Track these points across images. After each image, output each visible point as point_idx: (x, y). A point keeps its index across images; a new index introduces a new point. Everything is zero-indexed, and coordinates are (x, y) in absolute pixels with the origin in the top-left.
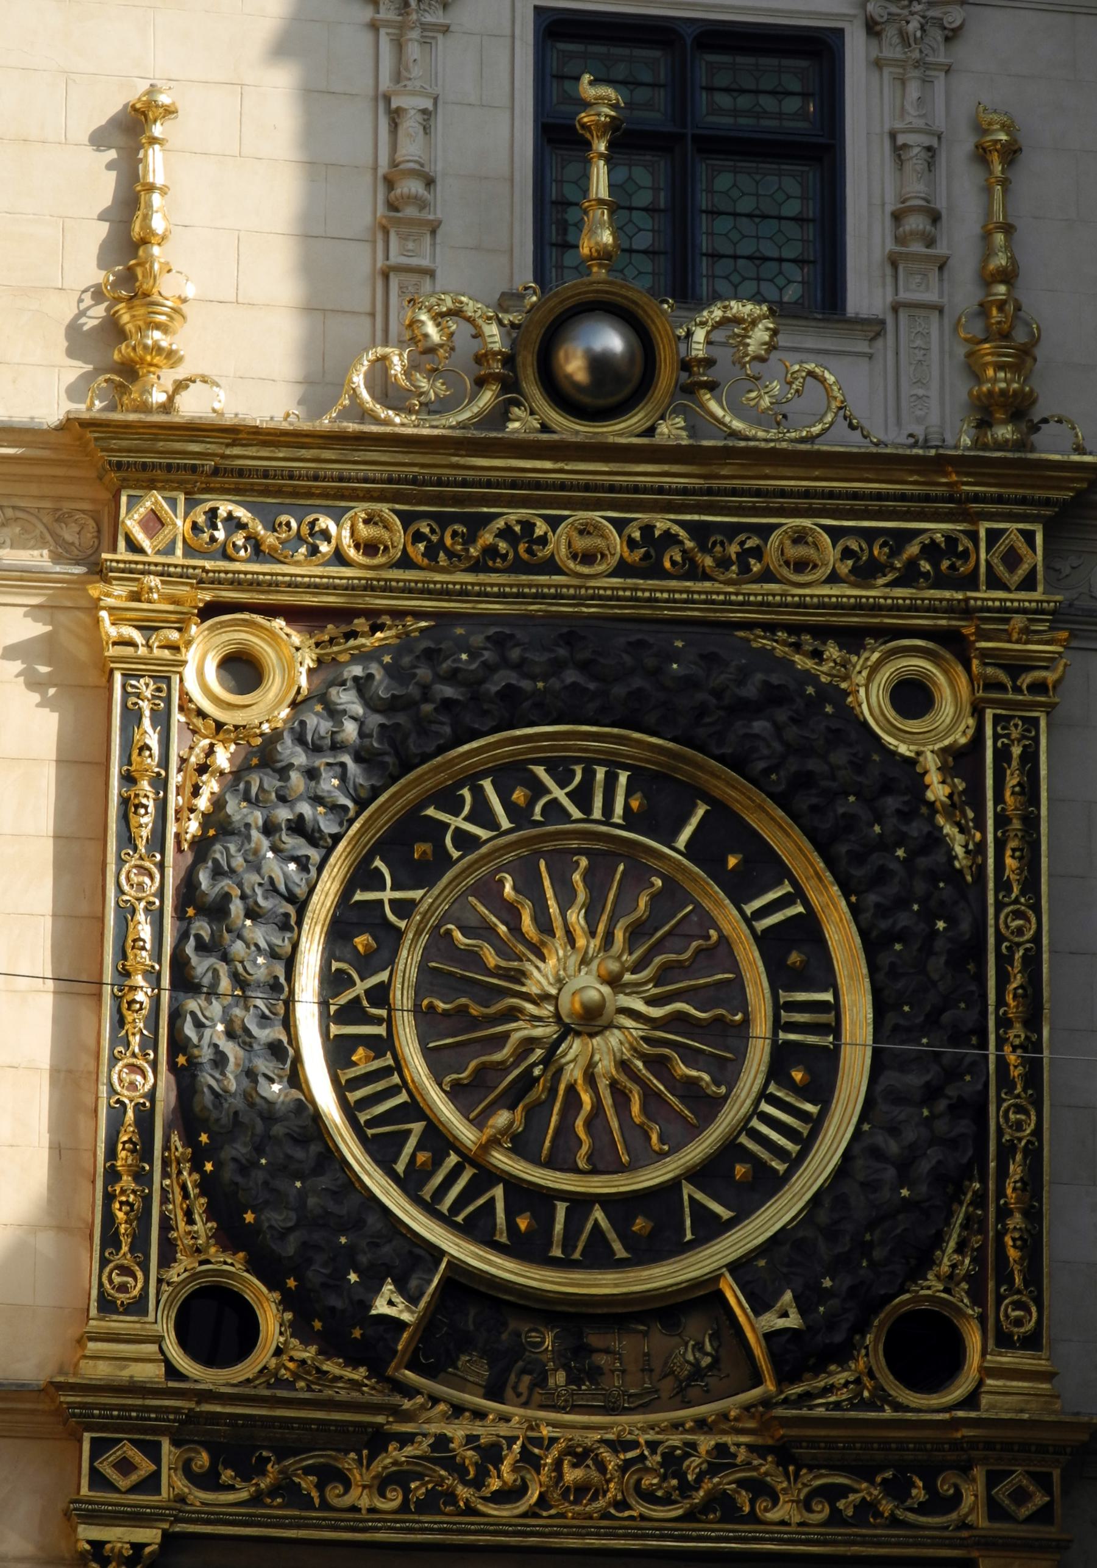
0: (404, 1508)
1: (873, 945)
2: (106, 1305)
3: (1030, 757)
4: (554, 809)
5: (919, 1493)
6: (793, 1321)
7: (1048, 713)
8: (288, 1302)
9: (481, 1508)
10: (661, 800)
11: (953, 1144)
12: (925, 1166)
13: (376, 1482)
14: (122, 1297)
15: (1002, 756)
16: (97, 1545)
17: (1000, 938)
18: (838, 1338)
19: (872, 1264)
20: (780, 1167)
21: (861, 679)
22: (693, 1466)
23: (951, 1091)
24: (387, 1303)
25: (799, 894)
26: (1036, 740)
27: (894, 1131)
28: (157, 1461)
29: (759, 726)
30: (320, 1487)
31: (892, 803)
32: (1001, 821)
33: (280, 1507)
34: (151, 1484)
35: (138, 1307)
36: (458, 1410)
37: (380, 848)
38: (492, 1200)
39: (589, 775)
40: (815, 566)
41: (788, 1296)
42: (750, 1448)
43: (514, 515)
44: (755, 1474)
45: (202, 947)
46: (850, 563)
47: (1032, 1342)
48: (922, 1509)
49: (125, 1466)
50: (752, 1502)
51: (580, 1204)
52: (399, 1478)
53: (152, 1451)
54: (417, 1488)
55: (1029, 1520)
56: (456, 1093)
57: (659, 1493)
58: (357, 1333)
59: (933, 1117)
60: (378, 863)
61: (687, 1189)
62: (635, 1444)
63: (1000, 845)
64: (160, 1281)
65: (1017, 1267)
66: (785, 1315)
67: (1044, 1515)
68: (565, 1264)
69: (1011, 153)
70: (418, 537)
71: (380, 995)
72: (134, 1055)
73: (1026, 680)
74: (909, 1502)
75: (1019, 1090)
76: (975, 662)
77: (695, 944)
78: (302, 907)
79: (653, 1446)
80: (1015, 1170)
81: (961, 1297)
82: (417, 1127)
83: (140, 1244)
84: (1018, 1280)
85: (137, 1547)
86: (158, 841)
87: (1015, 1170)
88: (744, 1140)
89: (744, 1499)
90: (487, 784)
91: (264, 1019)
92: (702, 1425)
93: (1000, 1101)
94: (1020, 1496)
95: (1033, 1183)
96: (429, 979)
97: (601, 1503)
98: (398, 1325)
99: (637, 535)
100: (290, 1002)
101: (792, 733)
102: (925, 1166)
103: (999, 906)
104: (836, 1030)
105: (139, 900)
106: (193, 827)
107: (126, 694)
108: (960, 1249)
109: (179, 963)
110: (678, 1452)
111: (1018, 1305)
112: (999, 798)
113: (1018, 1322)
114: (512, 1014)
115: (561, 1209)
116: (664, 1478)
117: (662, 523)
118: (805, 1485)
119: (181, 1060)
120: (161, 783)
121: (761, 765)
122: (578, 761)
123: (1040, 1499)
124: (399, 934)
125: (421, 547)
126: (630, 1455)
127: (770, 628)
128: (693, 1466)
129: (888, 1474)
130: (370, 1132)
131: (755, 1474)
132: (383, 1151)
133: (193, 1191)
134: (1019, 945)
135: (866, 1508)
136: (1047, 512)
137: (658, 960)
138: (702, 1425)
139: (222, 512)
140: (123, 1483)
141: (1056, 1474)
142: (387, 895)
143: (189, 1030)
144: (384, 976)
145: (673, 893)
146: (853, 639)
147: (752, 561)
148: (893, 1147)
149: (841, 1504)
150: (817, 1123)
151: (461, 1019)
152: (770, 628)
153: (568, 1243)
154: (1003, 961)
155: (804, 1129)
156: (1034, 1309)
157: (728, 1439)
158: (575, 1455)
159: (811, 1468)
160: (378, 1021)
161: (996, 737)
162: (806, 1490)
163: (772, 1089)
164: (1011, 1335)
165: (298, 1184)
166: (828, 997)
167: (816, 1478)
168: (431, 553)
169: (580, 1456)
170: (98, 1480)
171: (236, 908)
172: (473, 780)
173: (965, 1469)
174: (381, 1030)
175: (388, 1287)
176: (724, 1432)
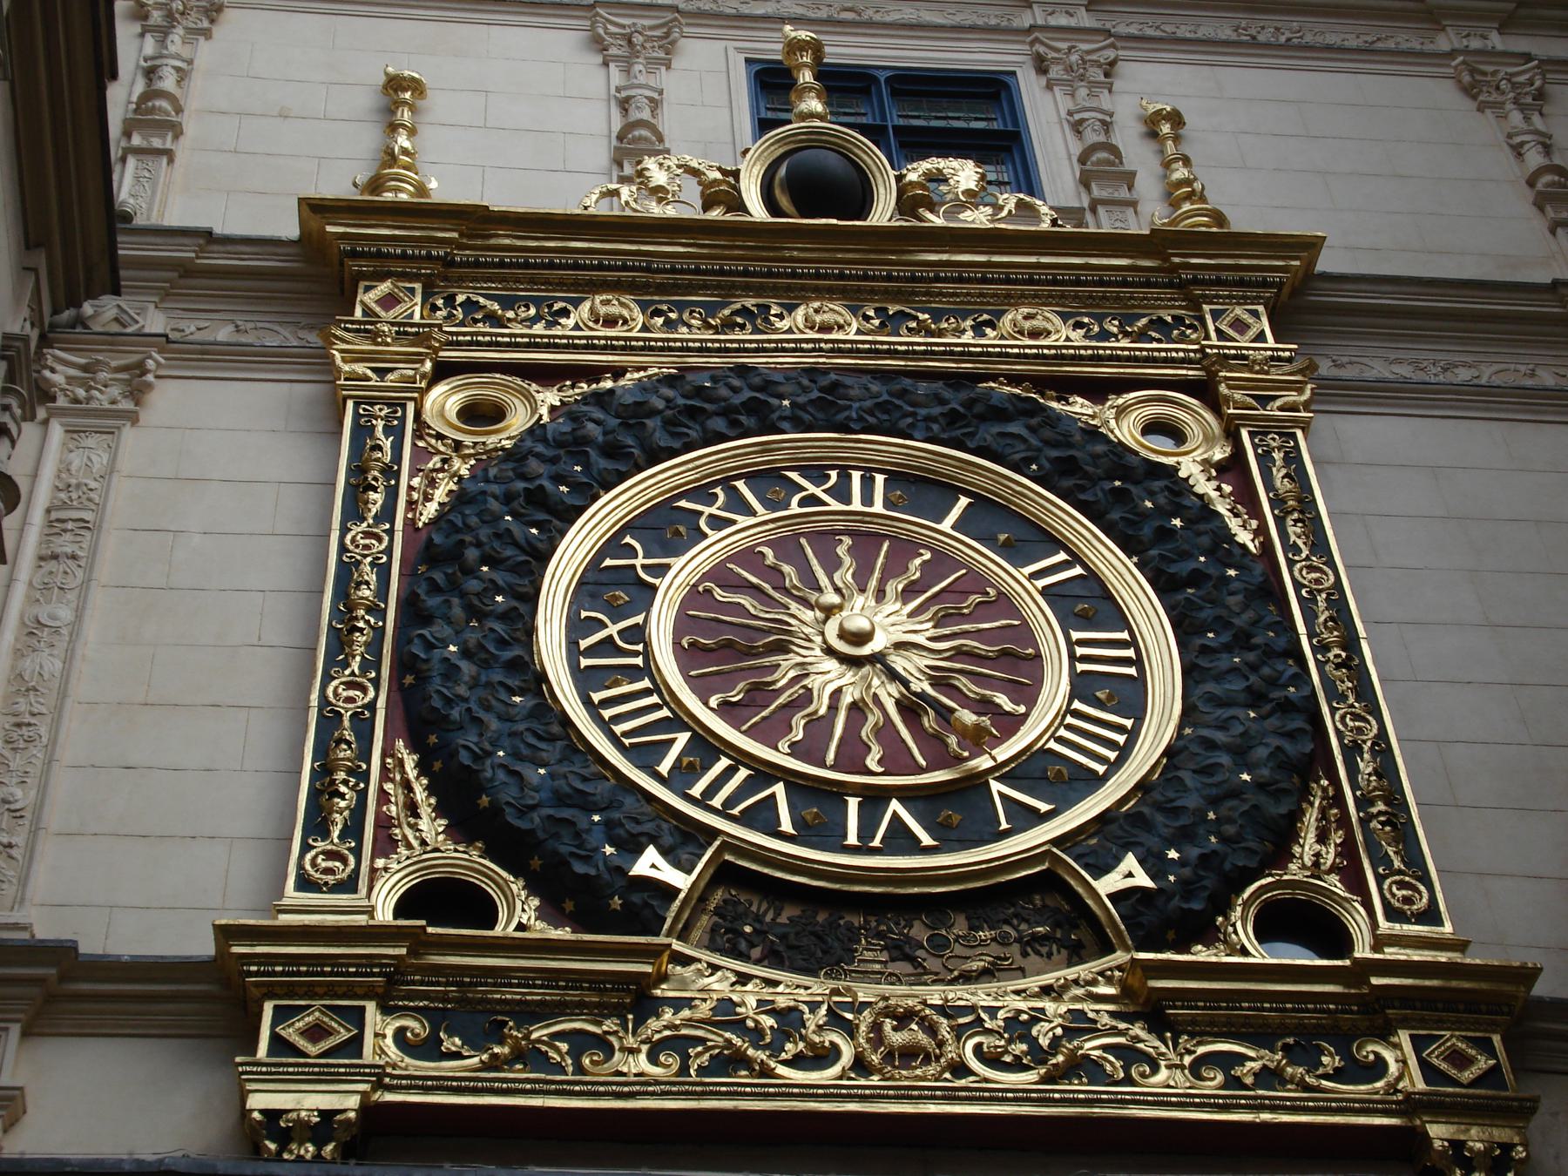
0: (684, 1070)
1: (1164, 584)
2: (305, 883)
3: (1293, 458)
4: (812, 500)
5: (1329, 1061)
6: (1143, 880)
7: (1303, 429)
8: (532, 888)
9: (781, 1070)
10: (920, 489)
11: (1291, 735)
12: (1261, 752)
13: (645, 1048)
14: (330, 879)
15: (1265, 459)
16: (272, 1115)
17: (1298, 586)
18: (1197, 906)
19: (1223, 839)
20: (1101, 769)
21: (1111, 414)
22: (1043, 1034)
23: (1276, 694)
24: (649, 863)
25: (1076, 558)
26: (1297, 447)
27: (1223, 726)
28: (361, 1025)
29: (1014, 428)
30: (576, 1055)
31: (1157, 485)
32: (1277, 502)
33: (519, 1071)
34: (354, 1046)
35: (349, 885)
36: (743, 979)
37: (627, 528)
38: (773, 796)
39: (845, 477)
40: (1049, 333)
41: (1130, 862)
42: (1112, 1014)
43: (750, 302)
44: (1122, 1040)
45: (435, 588)
46: (1081, 332)
47: (1431, 916)
48: (1337, 1075)
49: (316, 1032)
50: (1126, 1069)
51: (874, 799)
52: (678, 1044)
53: (357, 1017)
54: (699, 1055)
55: (1473, 1084)
56: (726, 710)
57: (1008, 1059)
58: (617, 902)
59: (1262, 718)
60: (628, 539)
61: (996, 786)
62: (972, 1009)
63: (1280, 522)
64: (373, 870)
65: (1390, 851)
66: (1130, 875)
67: (1491, 1077)
68: (863, 849)
69: (1176, 119)
70: (657, 313)
71: (637, 634)
72: (353, 673)
73: (1279, 403)
74: (1321, 1071)
75: (1351, 700)
76: (1223, 389)
77: (973, 597)
78: (544, 558)
79: (993, 1012)
80: (1365, 766)
81: (1334, 883)
82: (683, 738)
83: (353, 830)
84: (1397, 864)
85: (327, 1115)
86: (388, 513)
87: (1365, 766)
88: (1052, 745)
89: (1114, 1065)
90: (740, 484)
91: (503, 643)
92: (1046, 991)
93: (1333, 711)
94: (1460, 1060)
95: (1386, 770)
96: (684, 623)
97: (932, 1069)
98: (670, 892)
99: (871, 313)
100: (531, 631)
101: (1047, 433)
102: (1261, 752)
103: (1291, 564)
104: (1138, 662)
105: (365, 556)
106: (430, 510)
107: (357, 416)
108: (1322, 838)
109: (409, 604)
110: (1024, 1017)
111: (1402, 885)
112: (1269, 486)
113: (1408, 900)
114: (782, 648)
115: (853, 803)
116: (1010, 1041)
117: (892, 309)
118: (1190, 1052)
119: (409, 679)
120: (391, 472)
121: (1017, 457)
122: (833, 467)
123: (1483, 1063)
124: (654, 589)
125: (660, 321)
126: (961, 1021)
127: (1014, 379)
128: (1043, 1034)
129: (1290, 1040)
130: (627, 742)
131: (1122, 1040)
132: (646, 756)
133: (420, 794)
134: (1320, 591)
135: (1268, 1076)
136: (1268, 293)
137: (934, 609)
138: (1046, 991)
139: (460, 298)
140: (312, 1049)
141: (1496, 1039)
142: (639, 562)
143: (418, 650)
144: (639, 619)
145: (942, 561)
146: (1098, 390)
147: (988, 331)
148: (1220, 737)
149: (1237, 1071)
150: (1133, 735)
151: (727, 649)
152: (1014, 379)
153: (866, 831)
154: (1308, 606)
155: (1121, 739)
156: (1422, 888)
157: (1088, 1007)
158: (894, 1017)
159: (1192, 1035)
160: (636, 654)
161: (1255, 447)
162: (1187, 1060)
163: (1077, 705)
164: (1403, 912)
165: (542, 771)
166: (1125, 635)
167: (1200, 1043)
168: (669, 325)
169: (904, 1019)
170: (280, 1045)
171: (472, 554)
172: (727, 483)
173: (1384, 1034)
174: (639, 661)
175: (651, 854)
176: (1076, 999)
